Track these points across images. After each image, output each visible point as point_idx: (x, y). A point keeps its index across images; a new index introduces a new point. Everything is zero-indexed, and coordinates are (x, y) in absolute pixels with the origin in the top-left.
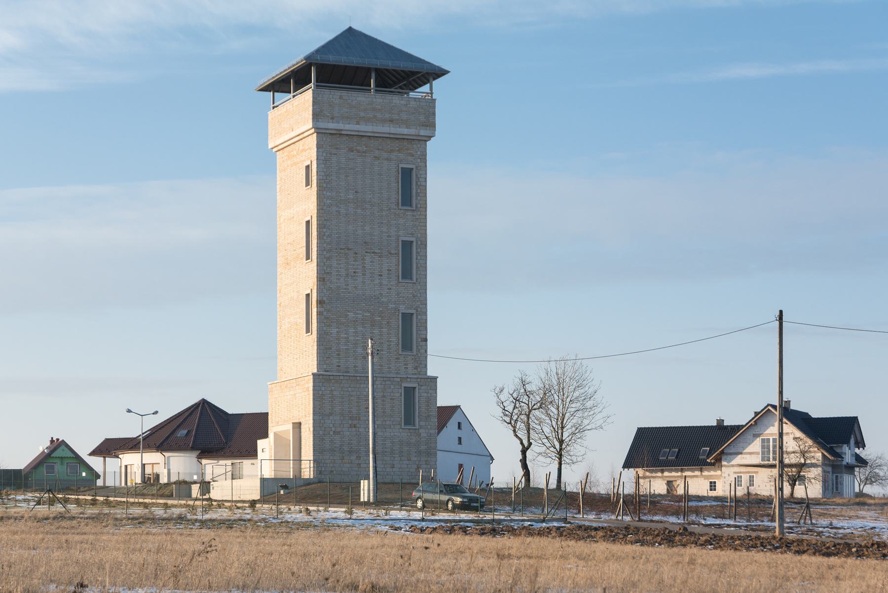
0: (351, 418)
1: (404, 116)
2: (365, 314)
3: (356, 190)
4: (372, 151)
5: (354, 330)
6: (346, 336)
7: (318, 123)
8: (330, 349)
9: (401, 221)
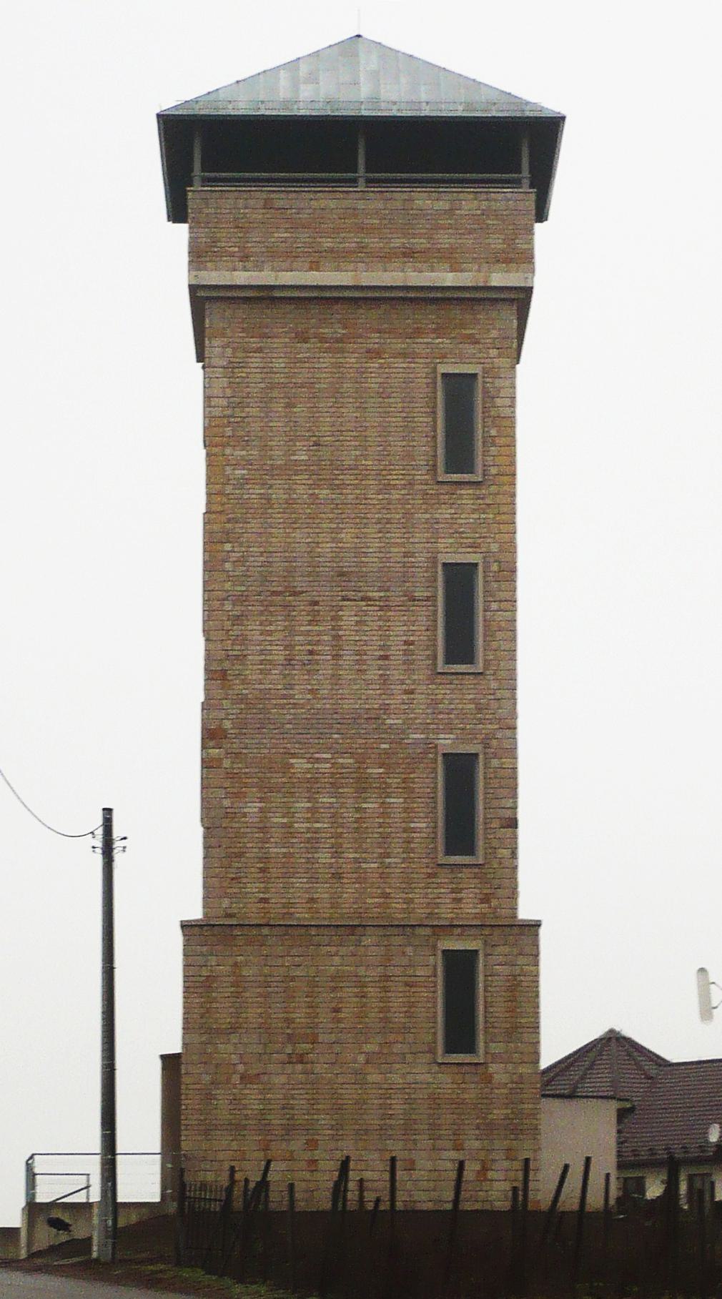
0: (290, 1038)
1: (445, 240)
2: (341, 761)
3: (314, 439)
4: (361, 337)
5: (309, 805)
6: (285, 820)
7: (203, 274)
8: (240, 855)
9: (445, 513)
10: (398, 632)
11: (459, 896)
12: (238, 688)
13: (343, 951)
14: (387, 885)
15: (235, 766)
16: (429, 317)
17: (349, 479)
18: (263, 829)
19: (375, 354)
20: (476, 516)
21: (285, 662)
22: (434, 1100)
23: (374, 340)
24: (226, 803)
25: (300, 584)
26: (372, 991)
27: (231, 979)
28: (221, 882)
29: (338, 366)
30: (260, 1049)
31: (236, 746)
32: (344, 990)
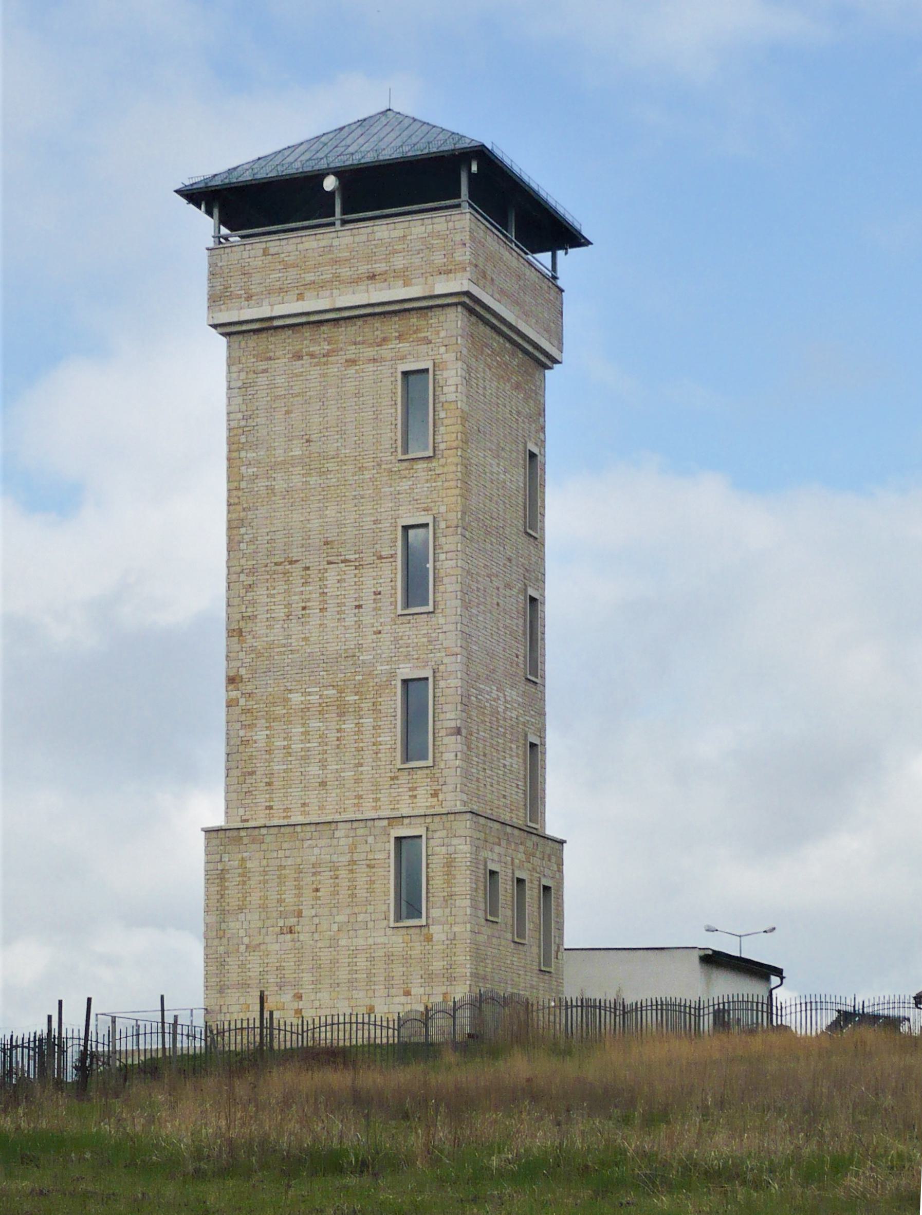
0: (281, 915)
1: (399, 262)
2: (325, 693)
3: (307, 437)
4: (341, 349)
5: (303, 729)
6: (286, 743)
8: (253, 773)
9: (405, 485)
10: (369, 585)
11: (415, 793)
12: (250, 640)
13: (322, 843)
14: (360, 789)
15: (247, 703)
16: (392, 327)
17: (331, 466)
18: (268, 752)
19: (352, 362)
20: (428, 485)
21: (285, 618)
22: (389, 957)
23: (351, 352)
24: (242, 733)
25: (295, 554)
26: (343, 873)
27: (240, 871)
28: (238, 796)
29: (324, 375)
30: (260, 924)
31: (249, 688)
32: (322, 874)
